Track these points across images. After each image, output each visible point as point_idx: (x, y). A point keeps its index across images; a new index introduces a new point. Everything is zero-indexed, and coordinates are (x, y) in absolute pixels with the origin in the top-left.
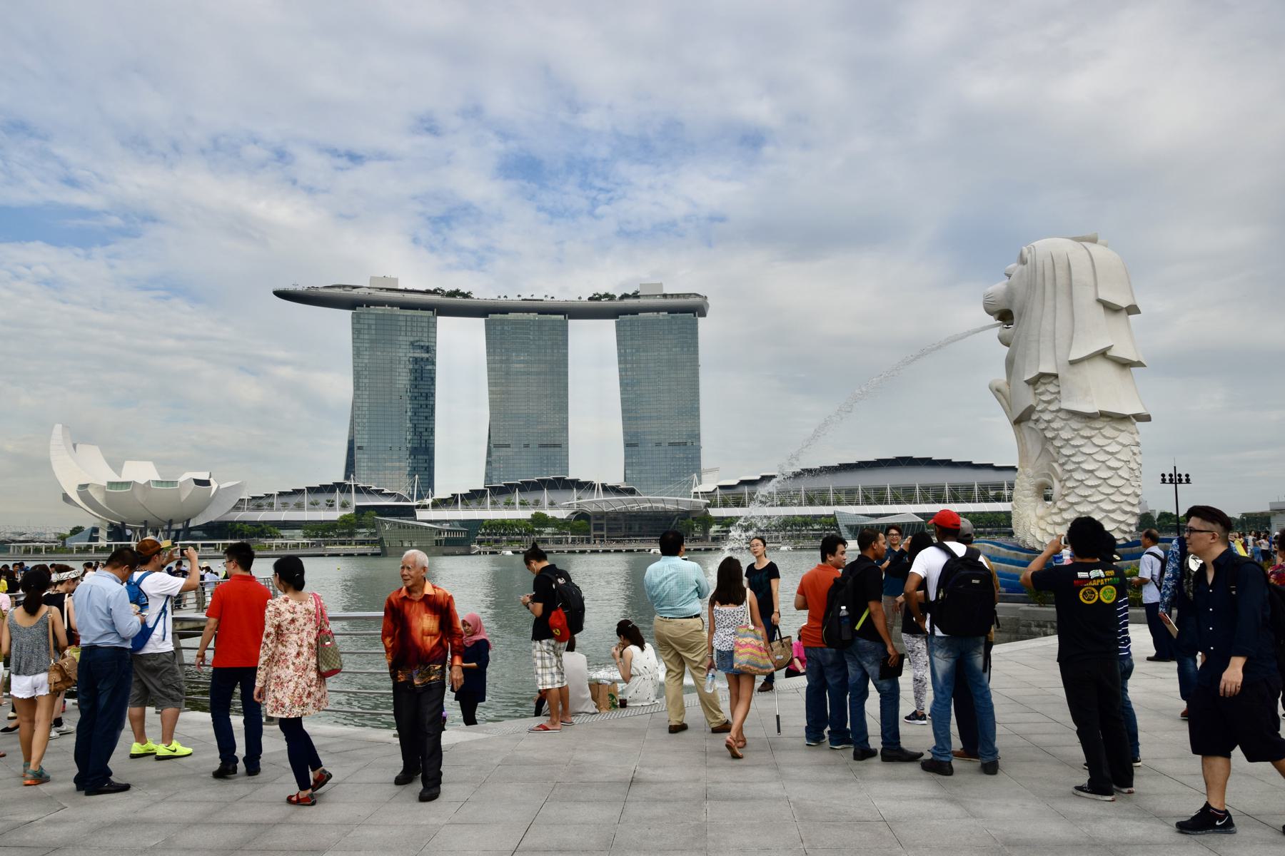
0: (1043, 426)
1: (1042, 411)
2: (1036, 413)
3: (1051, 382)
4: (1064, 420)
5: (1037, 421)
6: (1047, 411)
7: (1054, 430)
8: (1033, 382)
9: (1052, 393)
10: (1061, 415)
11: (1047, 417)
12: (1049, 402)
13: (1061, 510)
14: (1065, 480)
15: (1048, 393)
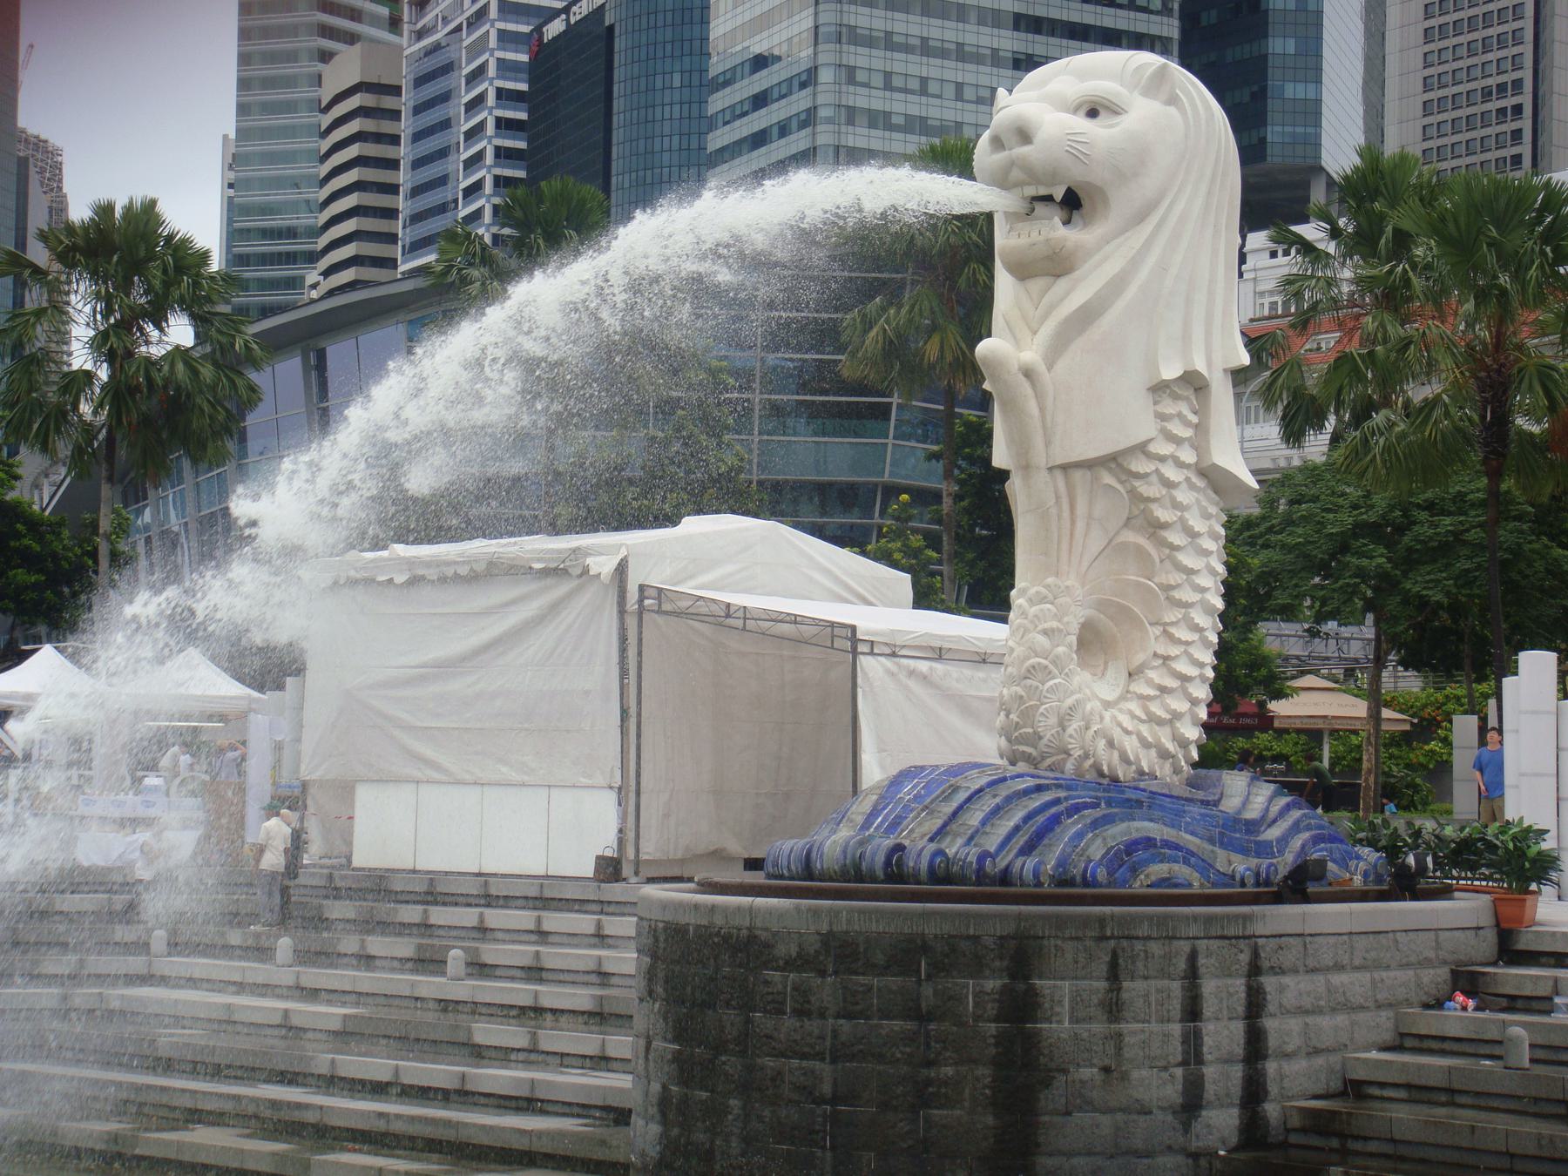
0: (1151, 490)
1: (1162, 459)
2: (1142, 457)
3: (1187, 399)
4: (1192, 486)
5: (1138, 476)
6: (1170, 462)
7: (1176, 505)
8: (1160, 389)
9: (1187, 423)
10: (1194, 479)
11: (1171, 473)
12: (1178, 441)
13: (1163, 690)
14: (1172, 624)
15: (1176, 420)
